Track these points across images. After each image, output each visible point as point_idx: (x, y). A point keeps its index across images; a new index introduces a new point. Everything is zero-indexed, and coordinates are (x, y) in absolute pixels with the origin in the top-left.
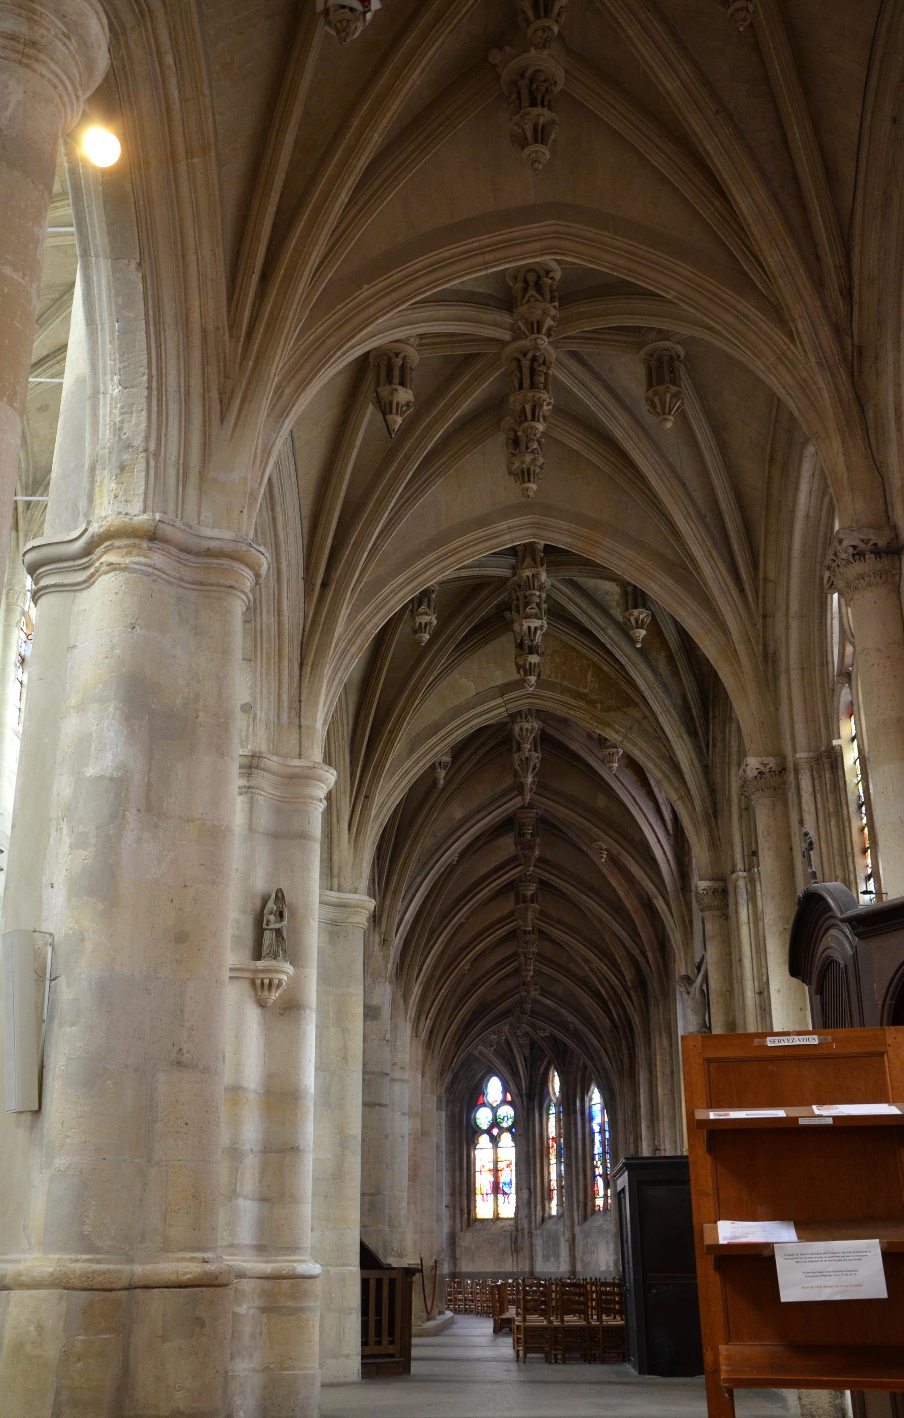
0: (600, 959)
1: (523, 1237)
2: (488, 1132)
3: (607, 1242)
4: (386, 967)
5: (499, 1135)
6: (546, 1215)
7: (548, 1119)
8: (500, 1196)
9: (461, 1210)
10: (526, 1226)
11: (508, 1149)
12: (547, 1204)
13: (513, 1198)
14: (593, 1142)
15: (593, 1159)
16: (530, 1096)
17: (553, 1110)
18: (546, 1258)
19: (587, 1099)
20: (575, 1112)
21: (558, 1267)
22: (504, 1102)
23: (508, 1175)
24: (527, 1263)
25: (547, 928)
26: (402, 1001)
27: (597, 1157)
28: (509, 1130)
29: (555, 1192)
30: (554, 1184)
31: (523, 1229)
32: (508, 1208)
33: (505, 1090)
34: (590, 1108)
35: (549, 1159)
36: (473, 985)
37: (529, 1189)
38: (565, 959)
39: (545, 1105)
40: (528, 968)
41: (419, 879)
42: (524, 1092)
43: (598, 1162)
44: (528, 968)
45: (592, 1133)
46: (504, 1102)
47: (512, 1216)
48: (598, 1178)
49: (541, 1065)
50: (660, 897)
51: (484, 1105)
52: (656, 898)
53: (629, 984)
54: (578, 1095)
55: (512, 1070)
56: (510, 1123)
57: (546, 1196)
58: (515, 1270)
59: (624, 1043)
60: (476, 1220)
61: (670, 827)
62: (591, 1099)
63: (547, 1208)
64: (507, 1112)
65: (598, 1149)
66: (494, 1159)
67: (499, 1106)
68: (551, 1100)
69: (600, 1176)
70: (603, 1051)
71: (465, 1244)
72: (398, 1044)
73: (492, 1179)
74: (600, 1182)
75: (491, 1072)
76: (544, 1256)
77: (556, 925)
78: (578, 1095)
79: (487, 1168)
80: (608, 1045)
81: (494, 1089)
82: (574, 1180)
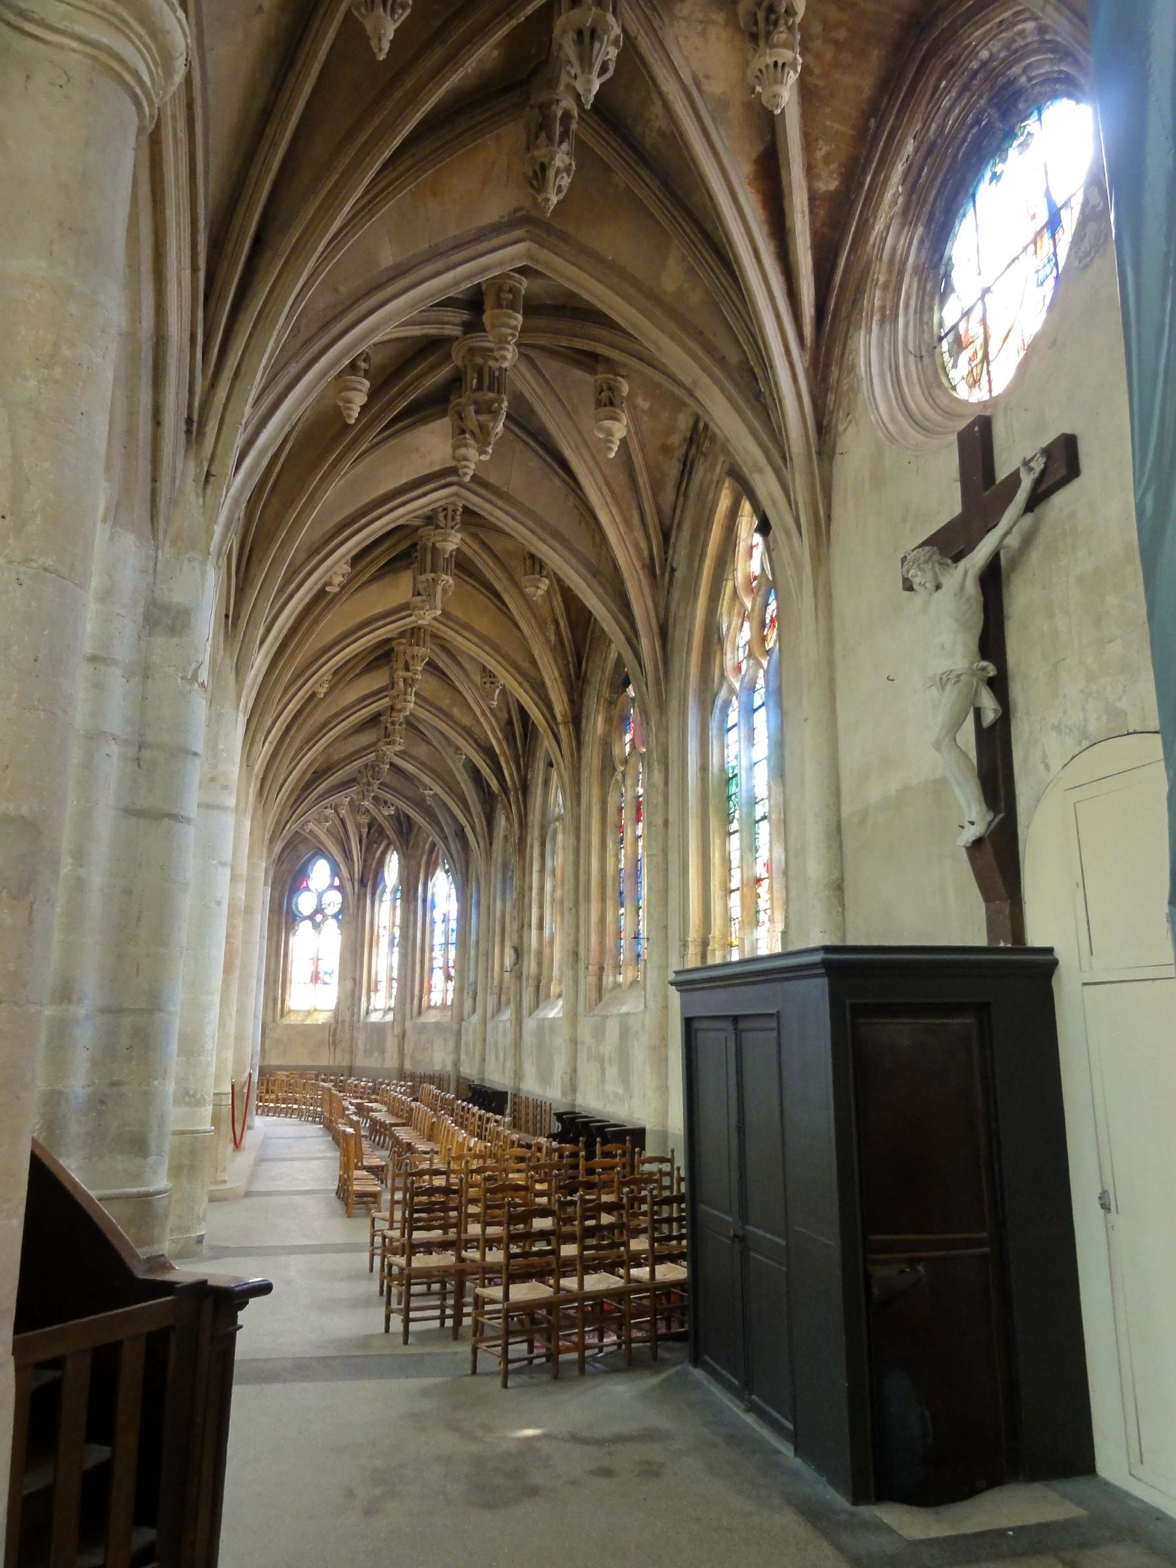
0: (520, 684)
1: (343, 1029)
3: (445, 1040)
4: (210, 533)
5: (323, 921)
6: (371, 1007)
8: (319, 986)
9: (275, 1000)
10: (348, 1019)
11: (331, 938)
12: (372, 994)
14: (432, 932)
15: (432, 950)
16: (363, 883)
17: (387, 897)
18: (368, 1053)
19: (430, 885)
20: (416, 900)
21: (383, 1063)
22: (332, 886)
23: (331, 962)
24: (347, 1057)
25: (447, 633)
26: (232, 676)
27: (437, 948)
28: (335, 916)
31: (343, 1021)
33: (335, 872)
34: (433, 895)
36: (324, 725)
37: (355, 980)
38: (447, 701)
40: (409, 698)
41: (294, 368)
42: (356, 876)
43: (438, 953)
45: (433, 922)
46: (332, 886)
47: (333, 1007)
49: (377, 849)
50: (768, 469)
51: (307, 888)
52: (760, 471)
53: (559, 718)
55: (345, 851)
56: (336, 909)
57: (372, 987)
58: (331, 1063)
59: (514, 809)
60: (290, 1011)
61: (808, 330)
62: (434, 886)
63: (372, 1000)
64: (334, 900)
65: (439, 939)
66: (315, 948)
68: (385, 886)
71: (276, 1036)
72: (221, 747)
73: (312, 968)
74: (438, 977)
75: (321, 852)
76: (366, 1051)
80: (476, 820)
82: (409, 972)
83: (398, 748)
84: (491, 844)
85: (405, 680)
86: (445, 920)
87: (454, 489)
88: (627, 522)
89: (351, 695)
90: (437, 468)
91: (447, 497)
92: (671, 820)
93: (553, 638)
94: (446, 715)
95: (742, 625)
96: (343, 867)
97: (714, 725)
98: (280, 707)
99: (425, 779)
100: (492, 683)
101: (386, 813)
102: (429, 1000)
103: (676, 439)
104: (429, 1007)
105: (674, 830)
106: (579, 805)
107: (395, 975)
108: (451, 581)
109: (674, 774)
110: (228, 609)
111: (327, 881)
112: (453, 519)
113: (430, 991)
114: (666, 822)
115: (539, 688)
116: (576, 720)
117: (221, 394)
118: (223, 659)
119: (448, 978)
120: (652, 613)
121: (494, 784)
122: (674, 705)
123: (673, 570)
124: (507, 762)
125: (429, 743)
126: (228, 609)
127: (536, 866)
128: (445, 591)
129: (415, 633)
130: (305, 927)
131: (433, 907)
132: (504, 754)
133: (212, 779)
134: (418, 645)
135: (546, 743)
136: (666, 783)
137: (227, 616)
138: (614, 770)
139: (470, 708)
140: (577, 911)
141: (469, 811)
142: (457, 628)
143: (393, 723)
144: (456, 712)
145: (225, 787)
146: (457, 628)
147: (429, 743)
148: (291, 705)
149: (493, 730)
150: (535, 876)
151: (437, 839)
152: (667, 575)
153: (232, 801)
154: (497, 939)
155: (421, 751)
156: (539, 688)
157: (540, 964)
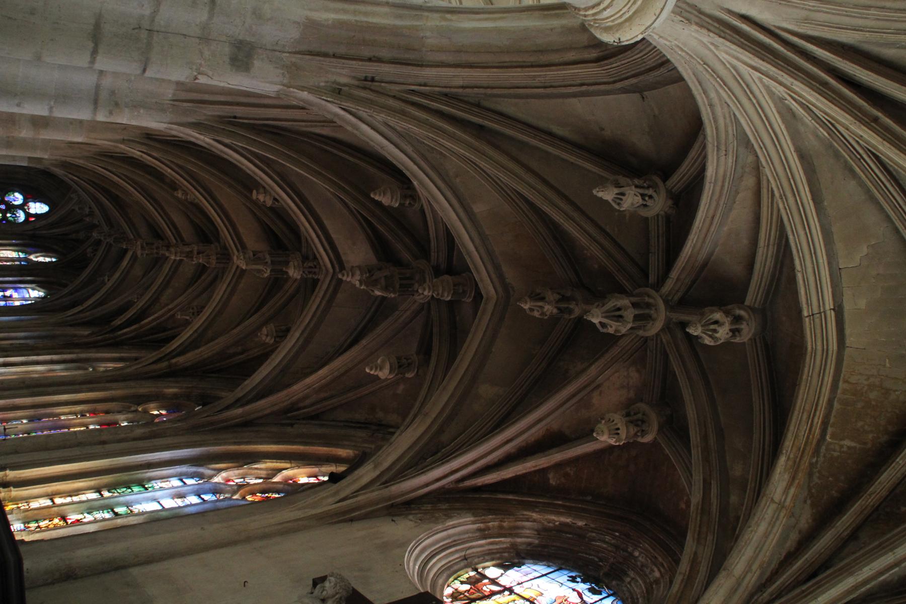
0: (196, 331)
4: (302, 88)
7: (14, 251)
19: (33, 286)
26: (194, 120)
40: (179, 254)
41: (409, 149)
44: (179, 254)
50: (377, 472)
52: (375, 467)
53: (174, 361)
54: (37, 279)
61: (468, 483)
62: (33, 289)
67: (24, 211)
70: (82, 308)
72: (142, 111)
77: (230, 288)
78: (37, 279)
80: (88, 313)
81: (38, 208)
83: (139, 253)
84: (71, 326)
85: (191, 252)
87: (331, 270)
88: (321, 389)
89: (177, 218)
90: (344, 258)
91: (325, 266)
92: (107, 446)
93: (231, 351)
94: (166, 284)
95: (260, 478)
96: (44, 222)
97: (184, 469)
98: (168, 163)
99: (117, 275)
100: (193, 314)
101: (89, 250)
103: (380, 415)
105: (98, 449)
106: (108, 382)
108: (266, 275)
109: (141, 444)
110: (240, 118)
111: (32, 211)
112: (310, 272)
114: (104, 443)
115: (193, 344)
116: (173, 374)
117: (391, 102)
118: (205, 115)
120: (260, 414)
121: (118, 322)
122: (196, 438)
123: (292, 425)
124: (135, 330)
125: (144, 276)
126: (240, 118)
127: (55, 357)
128: (259, 271)
129: (225, 256)
131: (16, 289)
132: (141, 327)
133: (117, 104)
134: (217, 259)
135: (154, 355)
136: (135, 439)
137: (235, 117)
138: (139, 404)
139: (172, 301)
140: (22, 388)
141: (95, 307)
142: (232, 285)
143: (157, 248)
144: (169, 291)
145: (111, 113)
146: (232, 285)
147: (144, 276)
148: (169, 170)
149: (158, 318)
151: (70, 288)
152: (288, 421)
153: (101, 117)
155: (138, 271)
156: (193, 344)
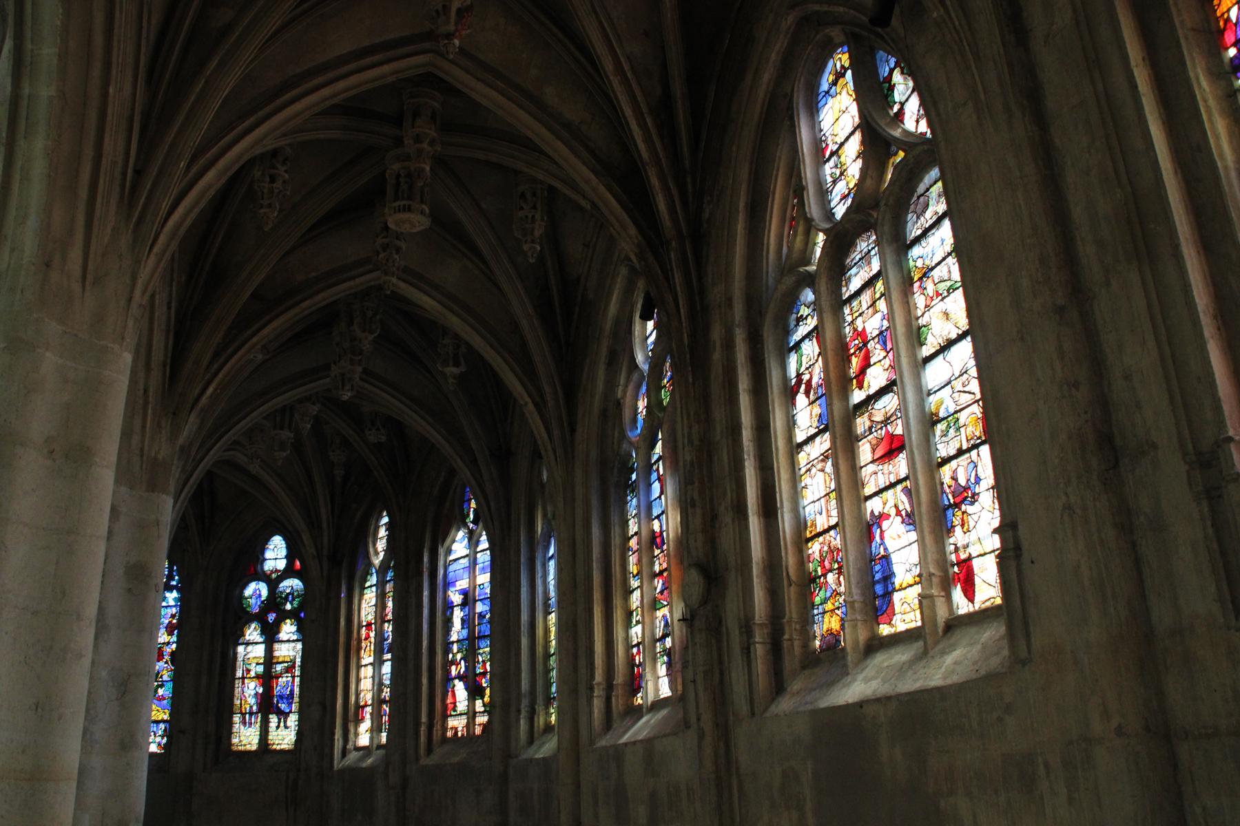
2: (260, 618)
6: (350, 746)
7: (362, 595)
13: (293, 720)
14: (448, 622)
19: (441, 551)
20: (420, 574)
23: (288, 683)
29: (369, 709)
30: (367, 697)
32: (284, 736)
35: (359, 658)
37: (324, 706)
39: (359, 574)
42: (325, 552)
48: (456, 681)
54: (427, 545)
62: (449, 551)
63: (351, 736)
65: (457, 631)
69: (460, 677)
70: (531, 406)
78: (427, 545)
79: (252, 674)
80: (547, 389)
81: (276, 554)
84: (573, 431)
86: (468, 599)
96: (306, 538)
101: (372, 437)
102: (445, 729)
104: (444, 739)
107: (386, 693)
111: (281, 565)
113: (445, 716)
119: (475, 691)
130: (253, 633)
131: (448, 584)
143: (418, 139)
150: (745, 401)
151: (459, 464)
154: (597, 596)
157: (774, 594)
